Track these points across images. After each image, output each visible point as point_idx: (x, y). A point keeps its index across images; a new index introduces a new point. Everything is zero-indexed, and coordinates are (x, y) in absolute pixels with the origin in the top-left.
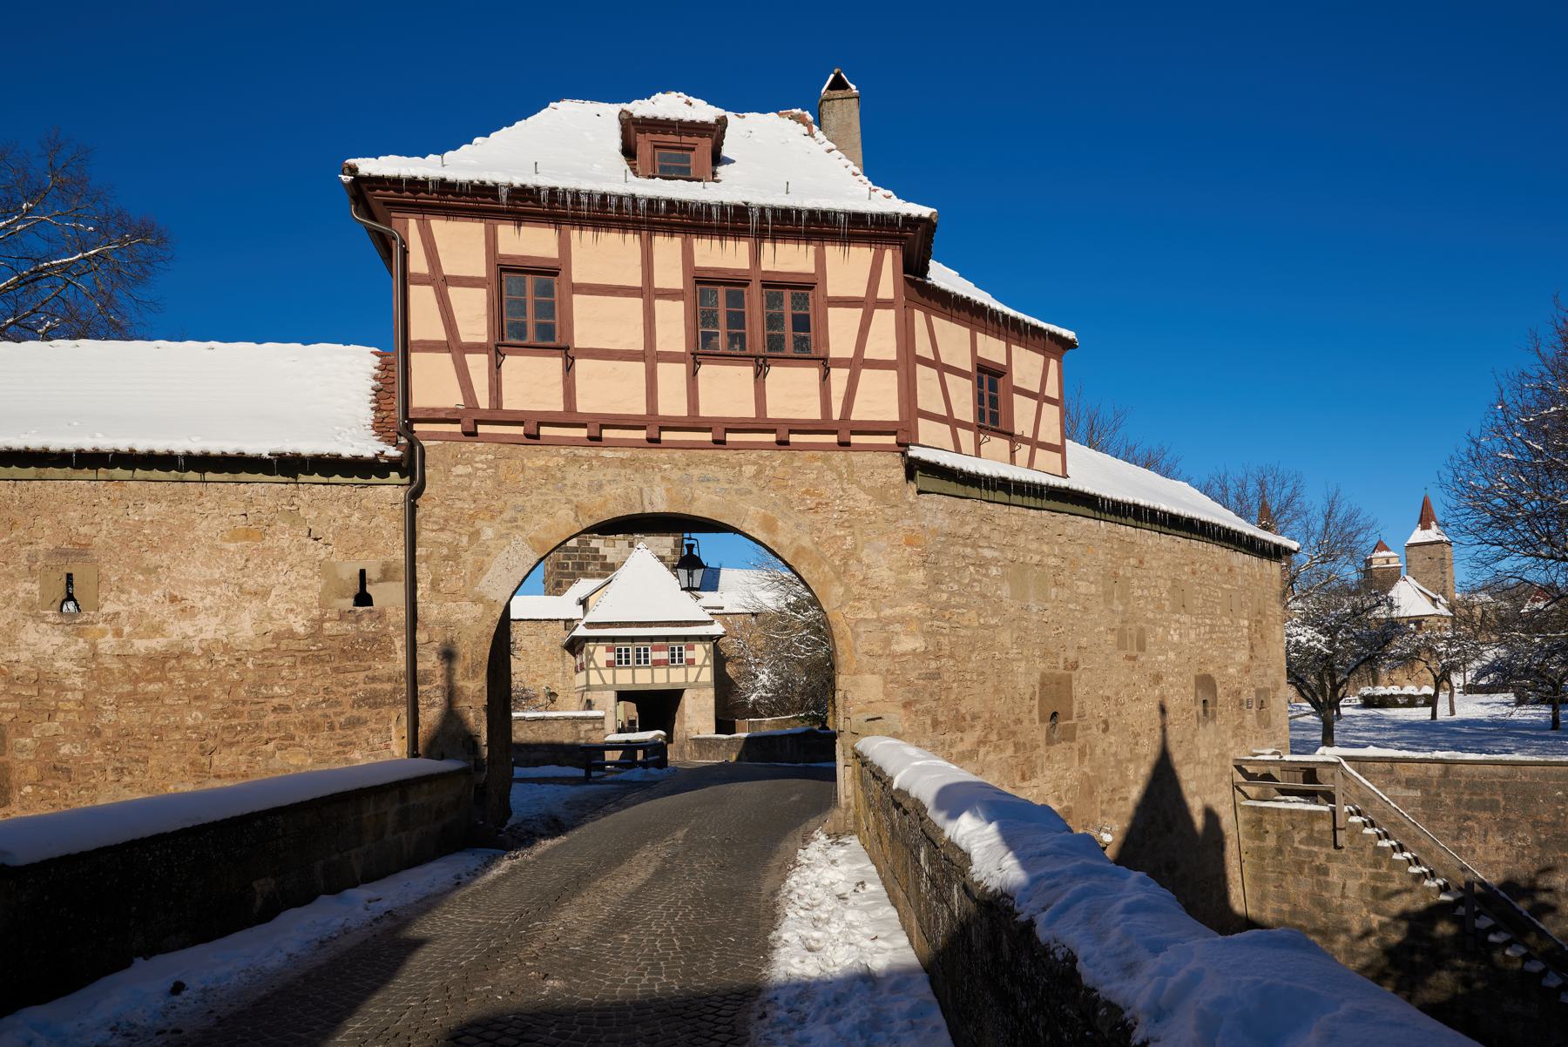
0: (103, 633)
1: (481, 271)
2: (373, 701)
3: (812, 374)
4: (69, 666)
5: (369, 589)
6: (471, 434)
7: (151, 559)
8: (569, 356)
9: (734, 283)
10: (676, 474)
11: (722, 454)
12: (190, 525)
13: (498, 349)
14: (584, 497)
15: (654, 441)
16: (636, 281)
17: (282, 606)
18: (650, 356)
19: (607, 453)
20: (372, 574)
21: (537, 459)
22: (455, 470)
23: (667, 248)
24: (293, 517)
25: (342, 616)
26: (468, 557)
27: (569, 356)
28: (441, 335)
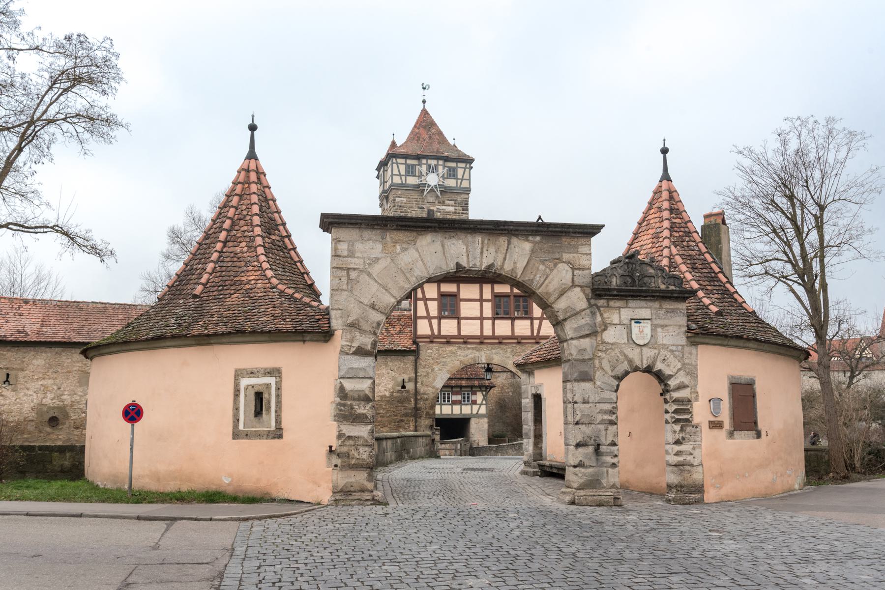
1: (436, 296)
2: (406, 415)
3: (528, 322)
6: (432, 342)
8: (459, 319)
9: (506, 296)
10: (488, 352)
13: (440, 318)
14: (462, 359)
16: (478, 297)
18: (481, 318)
19: (469, 346)
20: (406, 380)
22: (428, 352)
24: (386, 365)
25: (399, 391)
27: (459, 319)
28: (425, 314)
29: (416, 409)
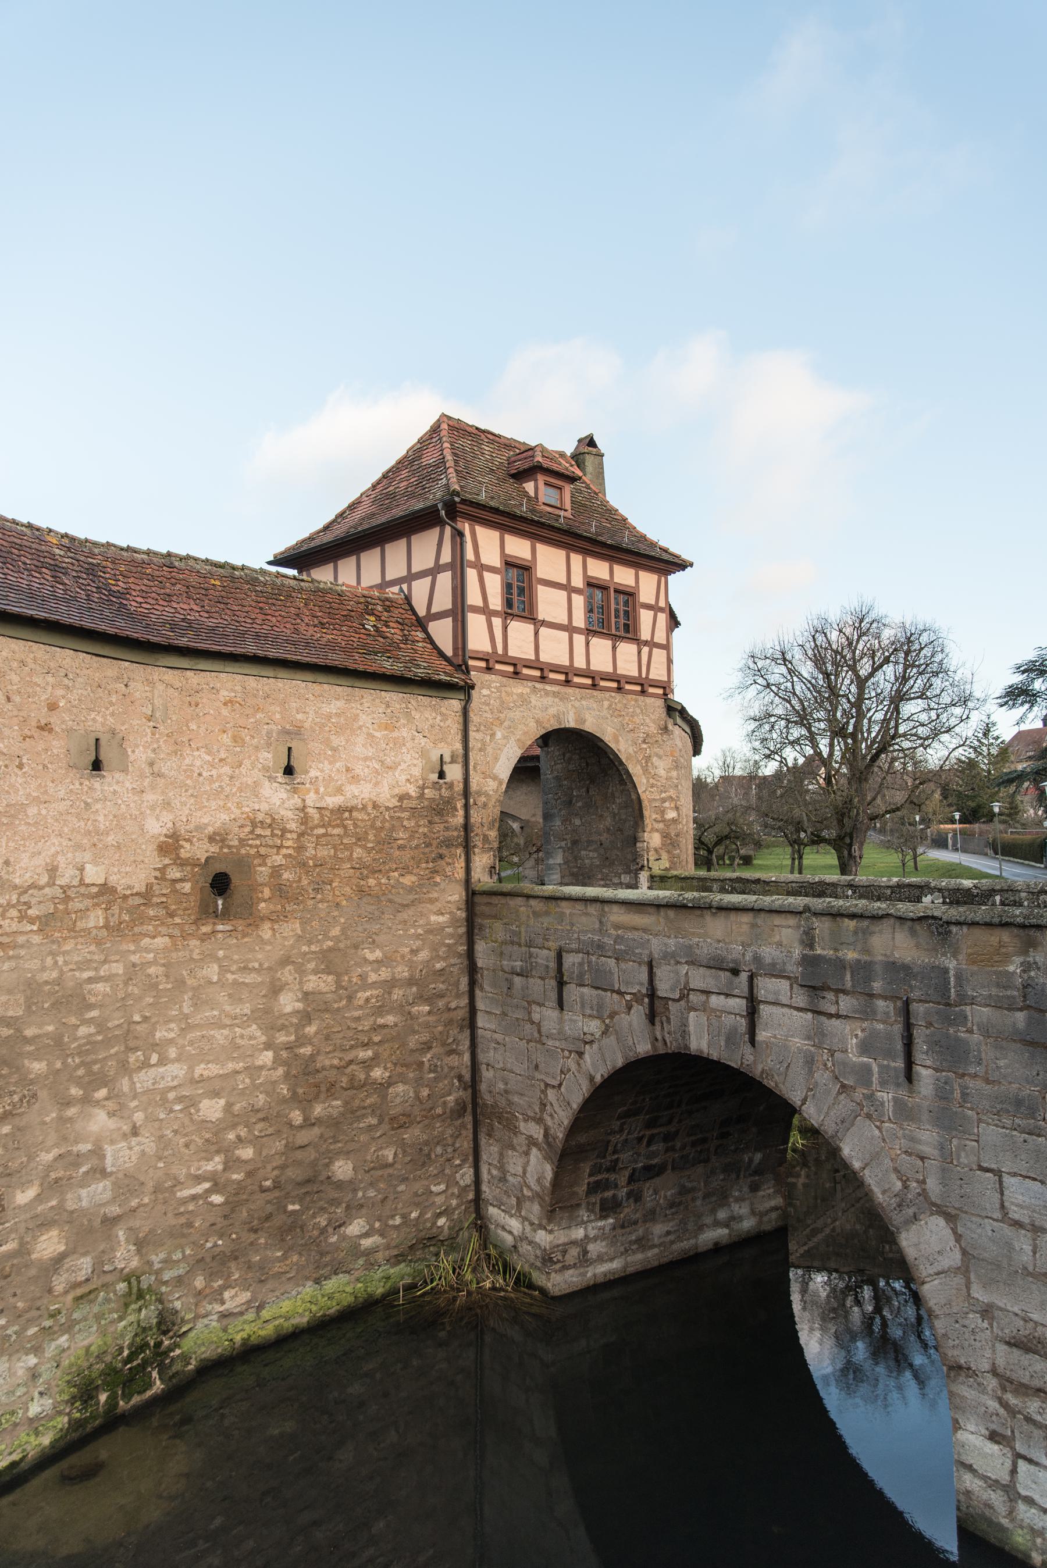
0: (308, 791)
3: (633, 648)
4: (289, 814)
5: (445, 768)
6: (489, 669)
7: (336, 741)
11: (595, 693)
12: (356, 718)
14: (539, 714)
15: (567, 682)
17: (403, 778)
19: (548, 687)
20: (447, 758)
21: (519, 689)
23: (576, 559)
26: (489, 749)
29: (467, 827)
